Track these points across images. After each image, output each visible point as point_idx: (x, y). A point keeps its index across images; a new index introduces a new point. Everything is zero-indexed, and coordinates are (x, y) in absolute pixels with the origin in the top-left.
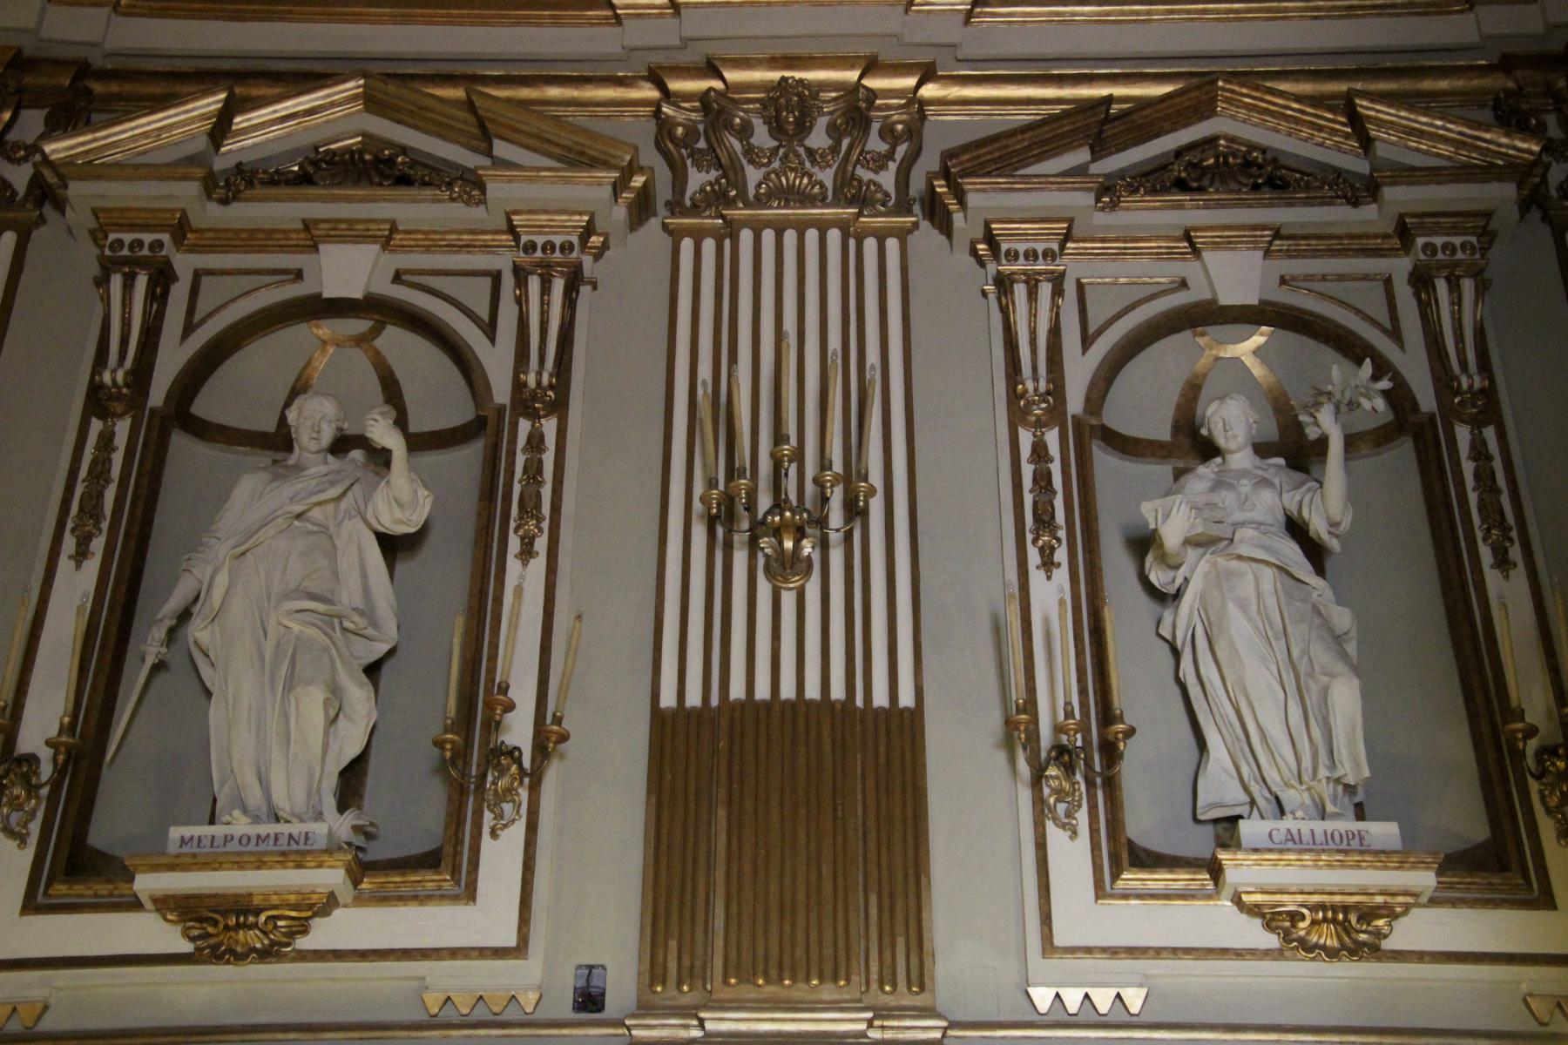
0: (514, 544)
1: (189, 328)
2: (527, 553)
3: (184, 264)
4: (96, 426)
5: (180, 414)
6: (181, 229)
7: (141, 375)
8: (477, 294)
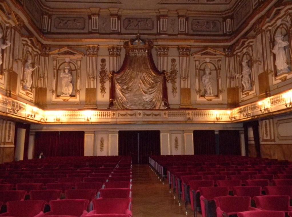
0: (78, 78)
1: (58, 64)
2: (79, 79)
3: (58, 59)
4: (54, 70)
5: (59, 69)
6: (57, 57)
7: (56, 67)
8: (75, 61)
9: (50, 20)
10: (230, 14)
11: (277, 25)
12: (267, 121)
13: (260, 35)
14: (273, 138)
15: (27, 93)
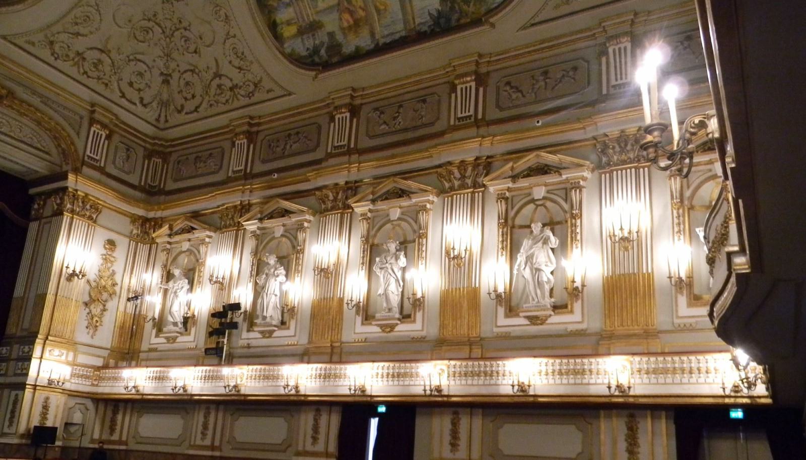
14: (217, 443)
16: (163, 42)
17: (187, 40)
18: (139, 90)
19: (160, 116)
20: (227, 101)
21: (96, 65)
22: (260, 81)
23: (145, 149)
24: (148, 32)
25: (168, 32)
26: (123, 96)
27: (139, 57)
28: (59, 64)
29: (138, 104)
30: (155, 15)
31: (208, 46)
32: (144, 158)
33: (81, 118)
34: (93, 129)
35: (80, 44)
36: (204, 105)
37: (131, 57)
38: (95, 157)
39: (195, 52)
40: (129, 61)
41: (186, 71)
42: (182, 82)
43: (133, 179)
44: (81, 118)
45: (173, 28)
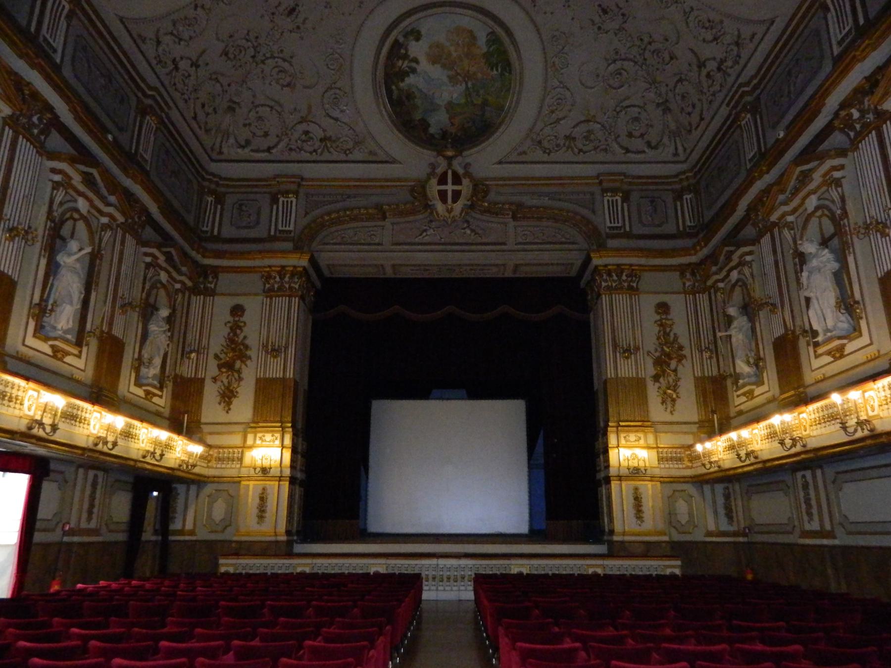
9: (219, 207)
10: (692, 181)
11: (806, 209)
12: (808, 474)
13: (769, 234)
15: (148, 393)
16: (640, 73)
17: (656, 52)
18: (642, 135)
19: (676, 149)
20: (721, 86)
21: (586, 138)
22: (739, 36)
23: (672, 190)
24: (620, 74)
25: (640, 59)
26: (628, 151)
27: (627, 103)
28: (553, 157)
29: (647, 150)
30: (617, 53)
31: (677, 43)
32: (675, 200)
33: (592, 194)
34: (606, 199)
35: (564, 128)
36: (705, 106)
37: (618, 109)
38: (616, 225)
39: (672, 58)
40: (618, 113)
41: (675, 87)
42: (678, 98)
43: (670, 228)
44: (592, 194)
45: (641, 52)
